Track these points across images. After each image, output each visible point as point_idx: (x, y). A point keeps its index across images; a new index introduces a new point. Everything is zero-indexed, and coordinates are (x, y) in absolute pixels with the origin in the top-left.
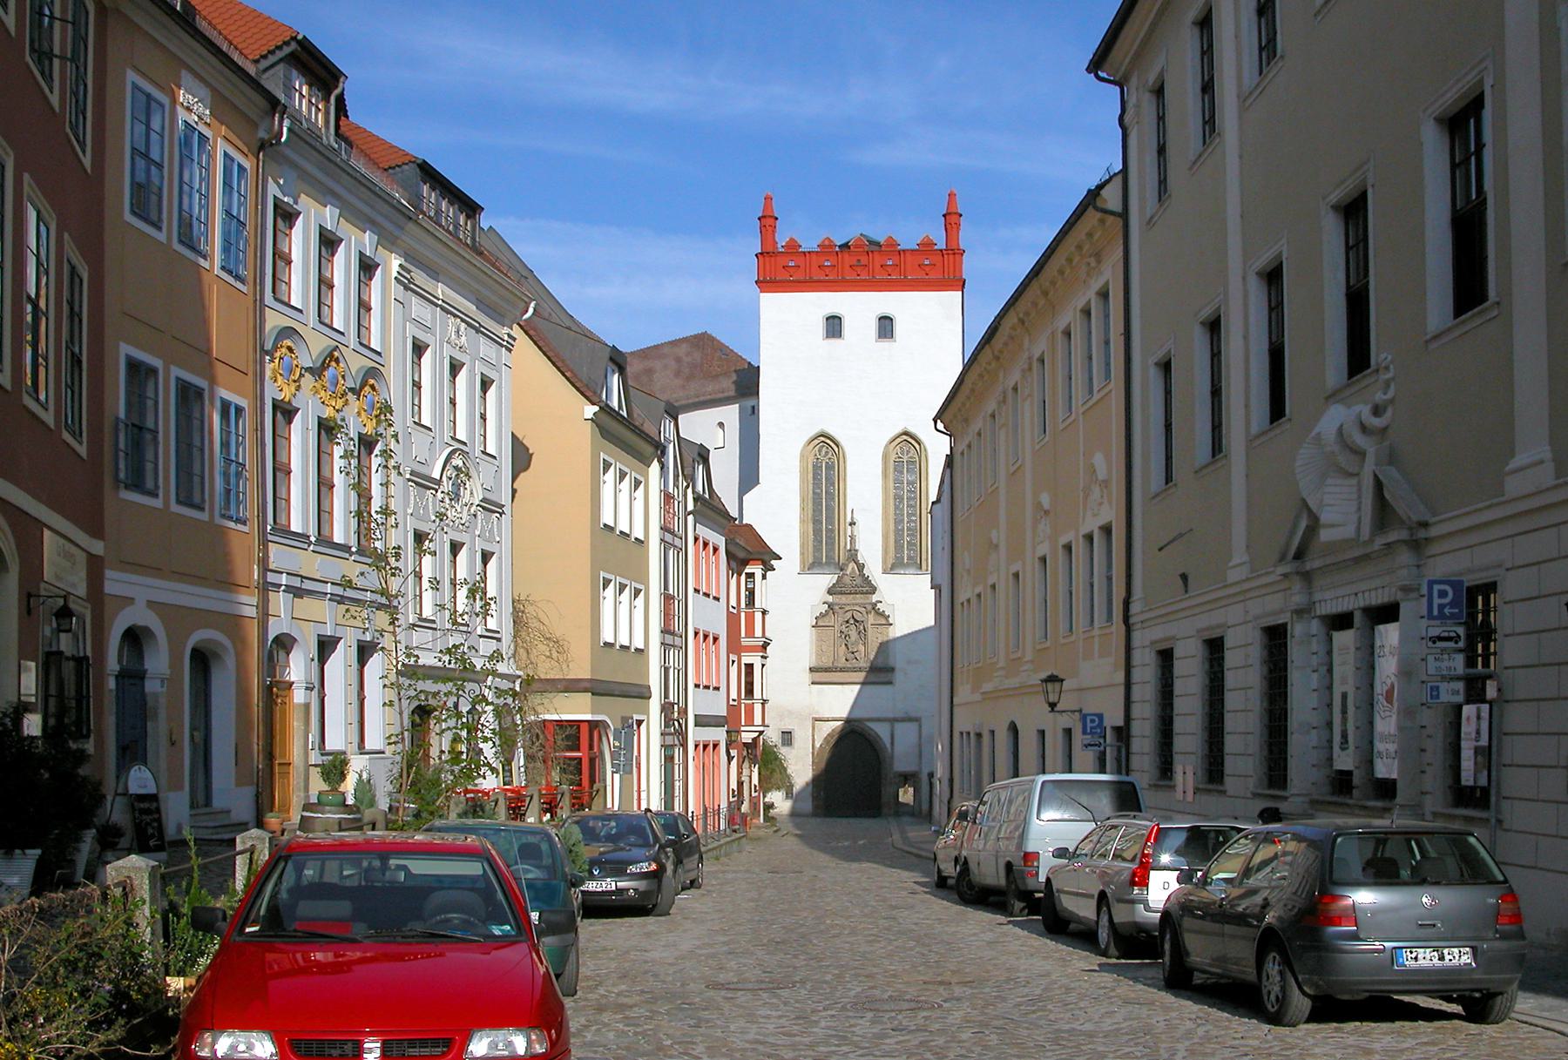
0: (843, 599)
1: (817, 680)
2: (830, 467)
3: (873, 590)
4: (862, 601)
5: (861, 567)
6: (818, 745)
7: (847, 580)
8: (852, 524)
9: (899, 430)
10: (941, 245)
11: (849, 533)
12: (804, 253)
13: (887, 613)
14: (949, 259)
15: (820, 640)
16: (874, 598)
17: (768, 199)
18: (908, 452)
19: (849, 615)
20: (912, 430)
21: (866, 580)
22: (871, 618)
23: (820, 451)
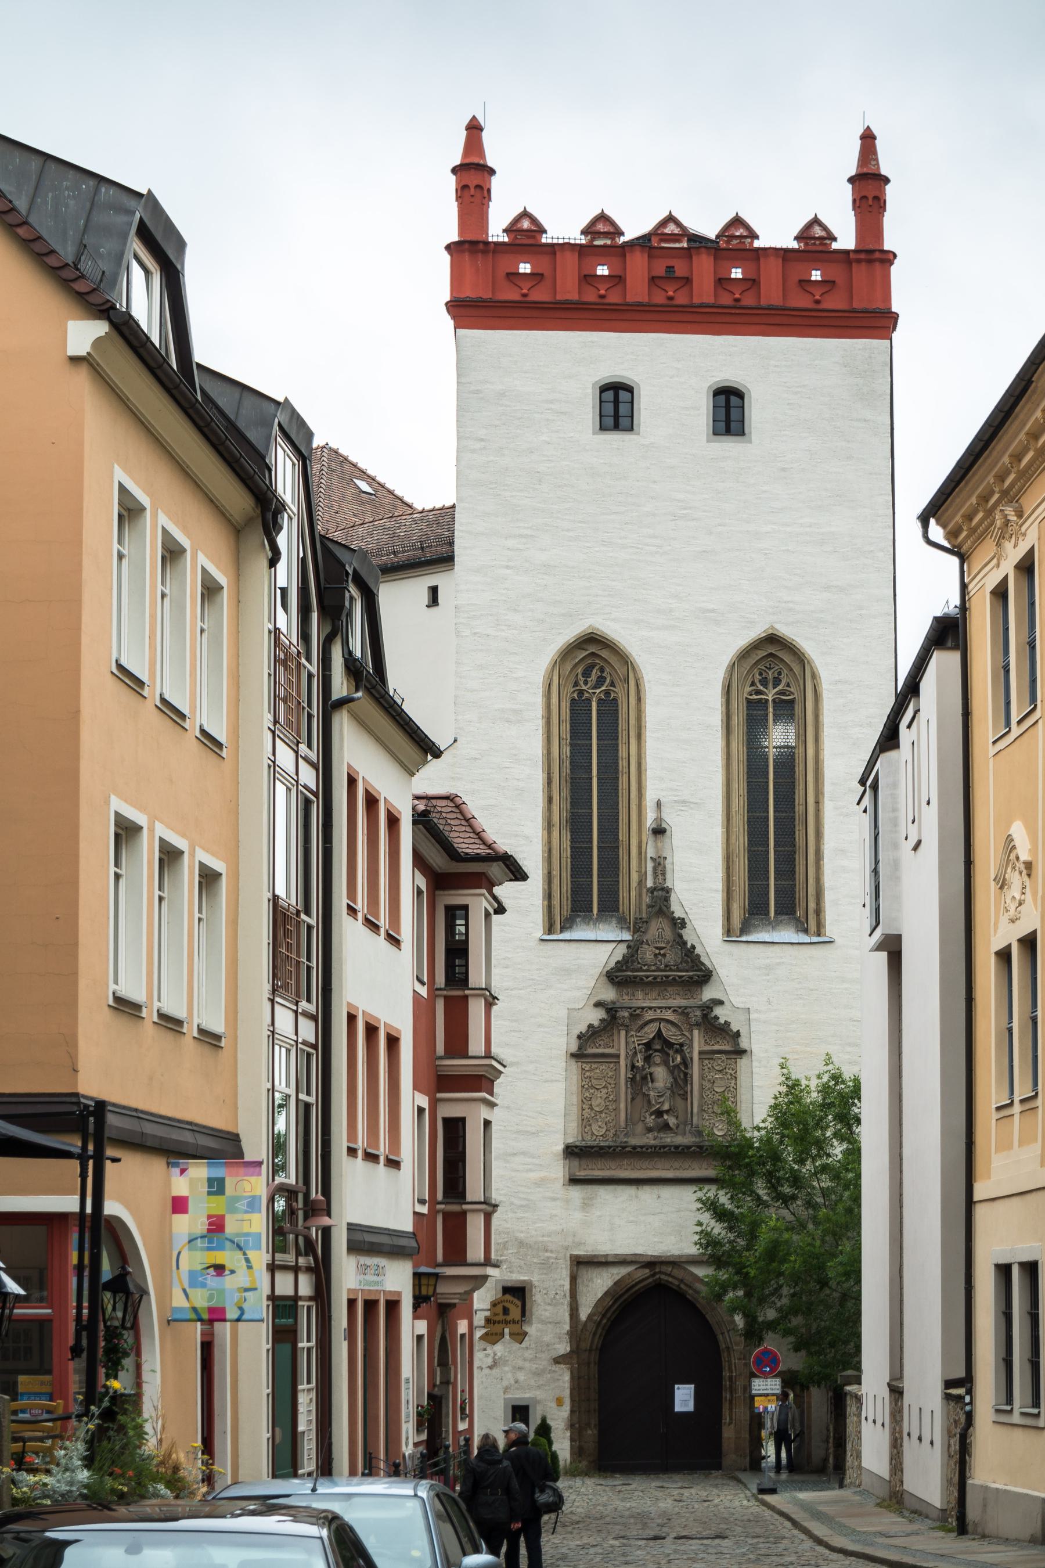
0: (641, 1000)
1: (581, 1174)
2: (610, 708)
3: (704, 976)
4: (683, 1003)
5: (679, 924)
6: (583, 1316)
7: (647, 954)
8: (659, 831)
9: (756, 632)
10: (846, 239)
11: (651, 852)
12: (553, 245)
13: (734, 1028)
14: (860, 272)
15: (587, 1087)
16: (708, 993)
17: (474, 128)
18: (777, 681)
19: (650, 1031)
20: (786, 631)
21: (690, 957)
22: (698, 1042)
23: (587, 673)
